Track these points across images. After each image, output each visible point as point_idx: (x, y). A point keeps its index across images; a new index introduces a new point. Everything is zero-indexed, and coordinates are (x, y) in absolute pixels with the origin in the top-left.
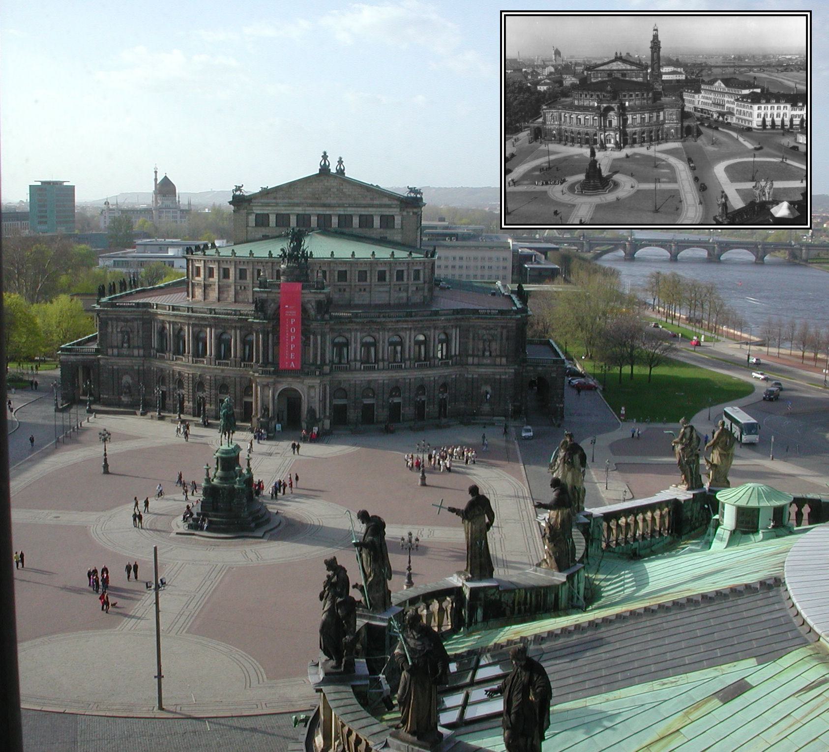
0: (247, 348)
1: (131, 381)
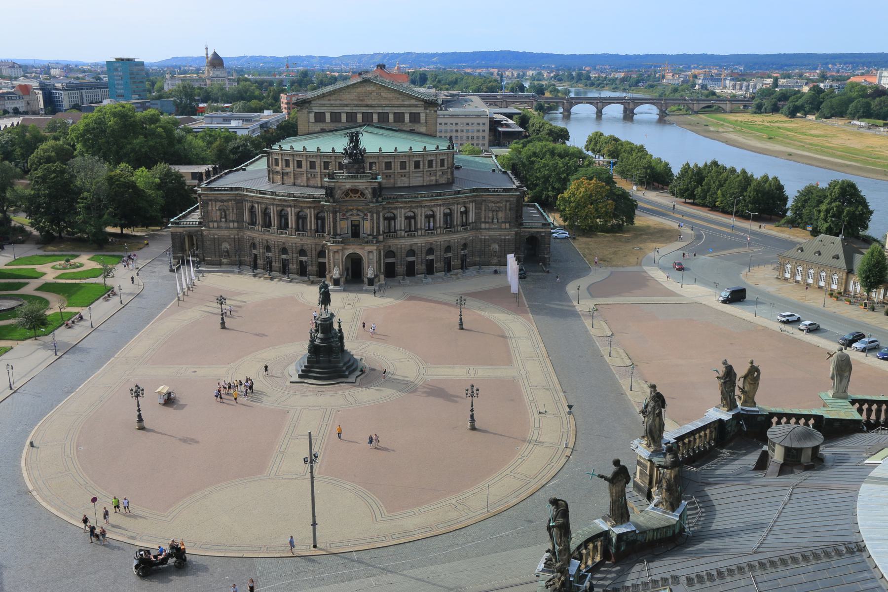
0: (319, 222)
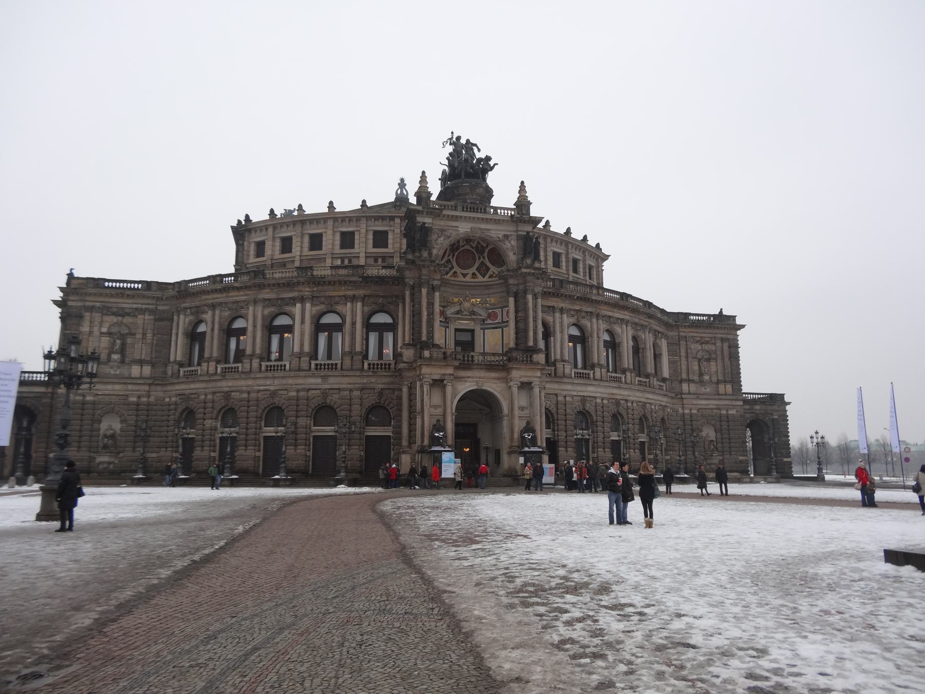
1: (117, 426)
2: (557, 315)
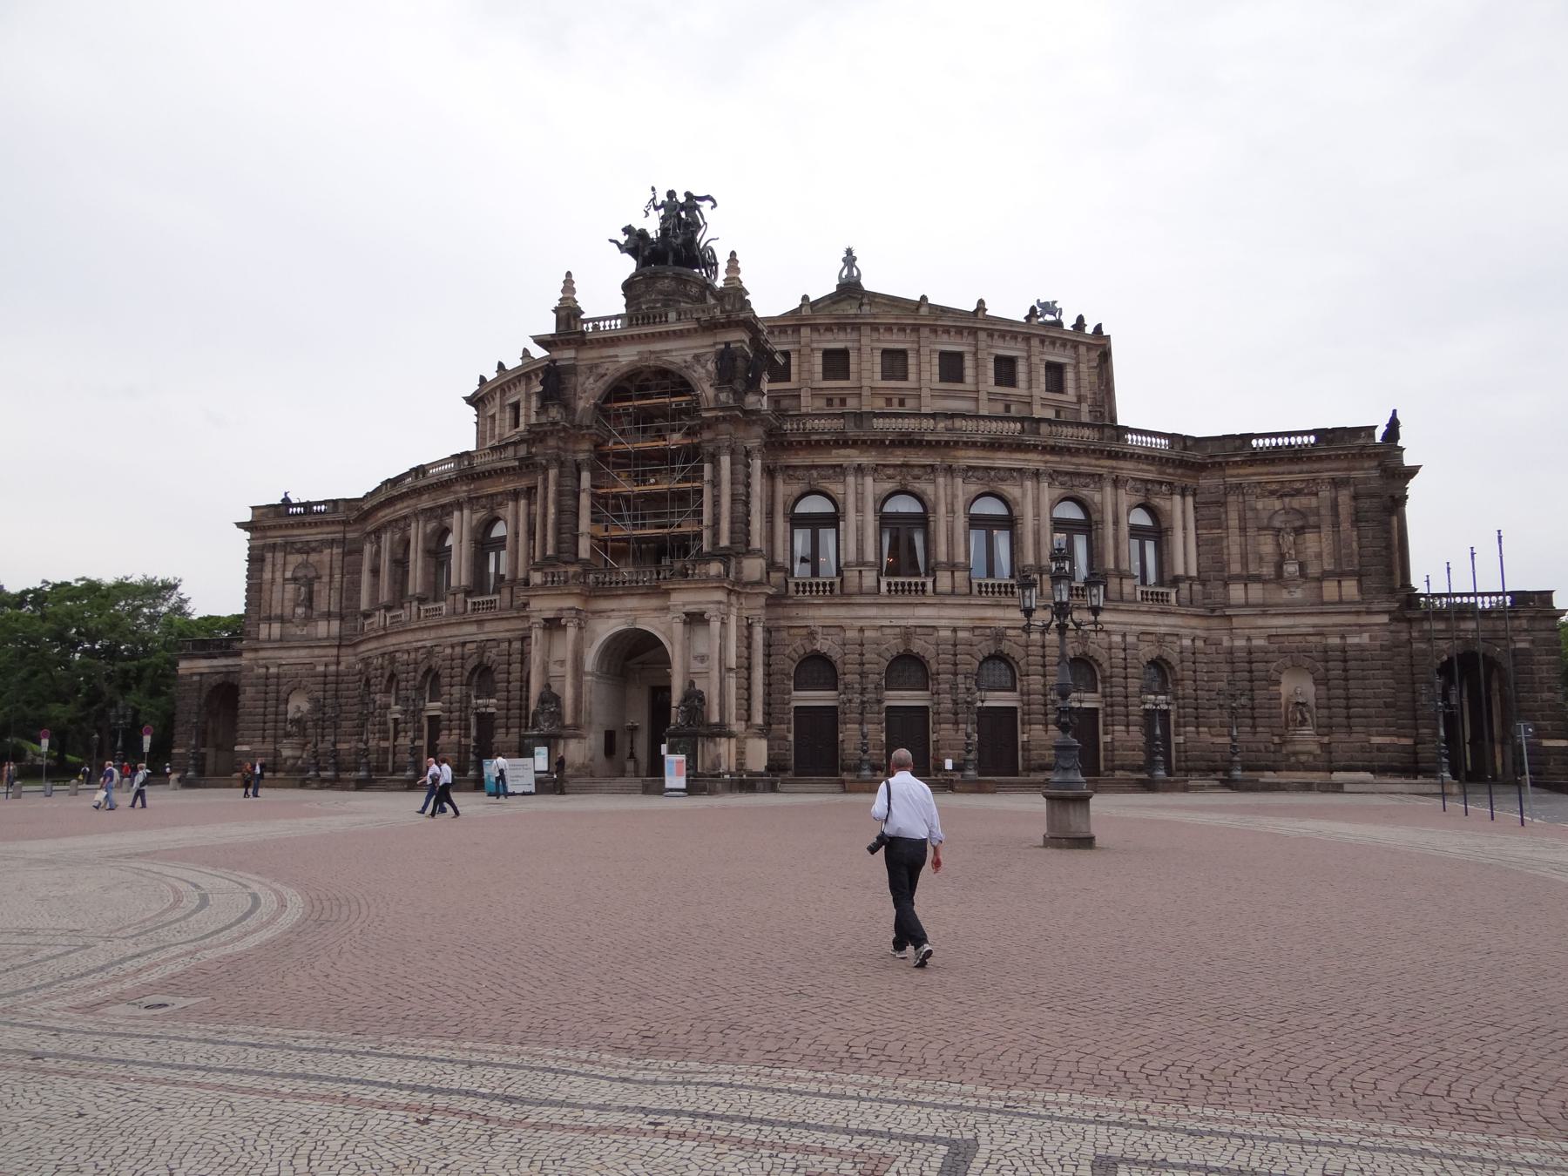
1: (305, 706)
2: (851, 480)
